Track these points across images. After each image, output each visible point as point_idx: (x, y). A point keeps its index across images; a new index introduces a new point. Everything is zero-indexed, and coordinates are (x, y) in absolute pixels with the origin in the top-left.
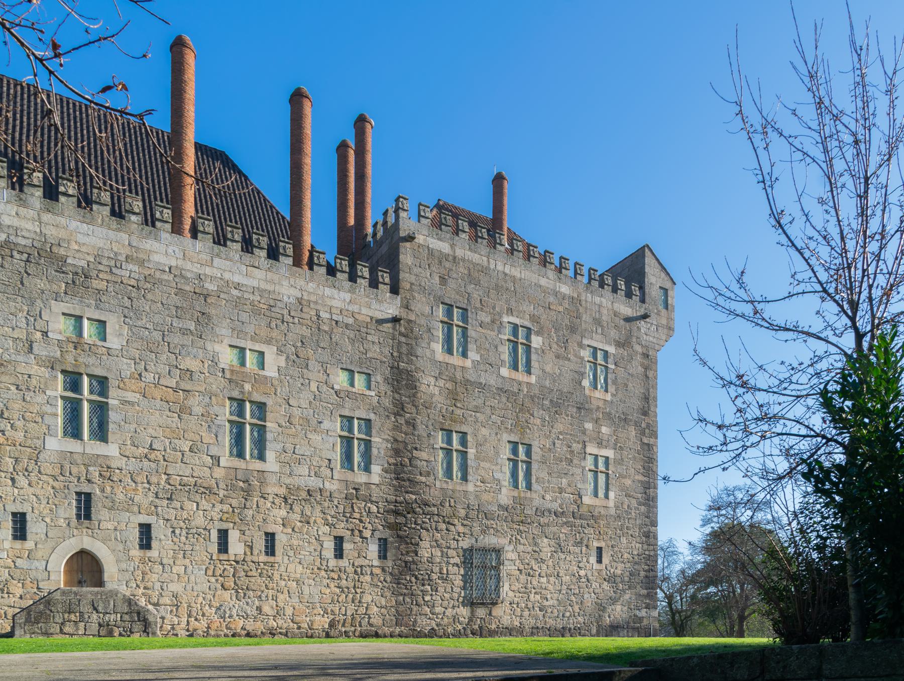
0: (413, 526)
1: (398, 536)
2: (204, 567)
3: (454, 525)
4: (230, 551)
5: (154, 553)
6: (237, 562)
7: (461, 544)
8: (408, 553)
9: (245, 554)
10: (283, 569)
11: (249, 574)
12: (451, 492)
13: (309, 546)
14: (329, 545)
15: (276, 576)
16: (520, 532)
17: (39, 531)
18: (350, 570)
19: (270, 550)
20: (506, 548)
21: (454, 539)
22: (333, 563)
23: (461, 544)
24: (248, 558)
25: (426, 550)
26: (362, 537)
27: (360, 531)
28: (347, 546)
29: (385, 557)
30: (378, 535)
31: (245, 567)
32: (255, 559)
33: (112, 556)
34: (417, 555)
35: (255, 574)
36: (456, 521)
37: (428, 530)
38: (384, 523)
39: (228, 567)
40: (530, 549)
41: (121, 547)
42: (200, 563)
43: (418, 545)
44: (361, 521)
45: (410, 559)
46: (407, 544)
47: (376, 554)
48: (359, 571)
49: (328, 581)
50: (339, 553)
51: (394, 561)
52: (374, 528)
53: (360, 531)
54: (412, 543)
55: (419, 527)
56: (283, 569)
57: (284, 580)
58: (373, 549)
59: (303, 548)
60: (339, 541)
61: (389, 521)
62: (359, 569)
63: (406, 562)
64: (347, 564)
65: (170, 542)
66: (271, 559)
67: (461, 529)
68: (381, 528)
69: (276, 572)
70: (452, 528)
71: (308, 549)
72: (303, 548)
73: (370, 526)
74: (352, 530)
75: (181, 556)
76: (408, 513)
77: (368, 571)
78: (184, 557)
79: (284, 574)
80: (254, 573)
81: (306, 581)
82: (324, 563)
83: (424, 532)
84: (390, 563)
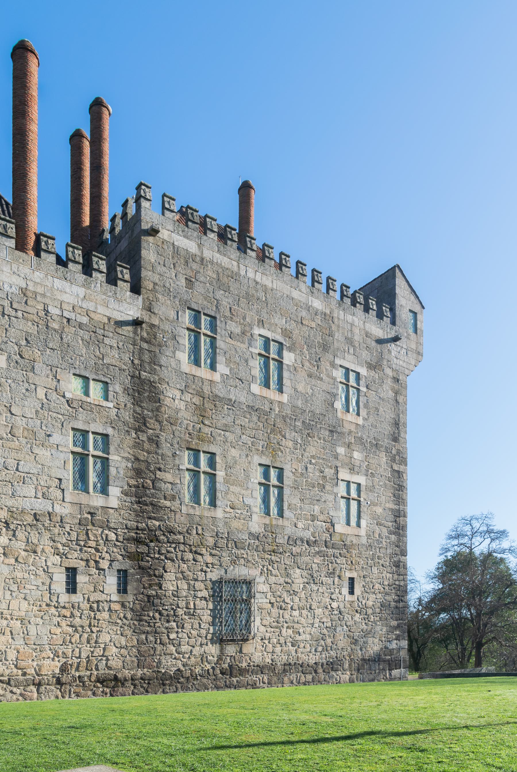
0: (157, 556)
1: (140, 567)
3: (202, 555)
7: (209, 575)
8: (150, 585)
12: (198, 519)
13: (36, 579)
14: (60, 578)
16: (271, 562)
18: (85, 606)
20: (258, 580)
21: (202, 570)
22: (64, 598)
23: (209, 575)
25: (171, 582)
26: (98, 569)
27: (96, 562)
28: (81, 579)
29: (125, 591)
30: (116, 566)
34: (161, 588)
36: (204, 551)
37: (173, 561)
38: (124, 553)
40: (282, 580)
43: (162, 577)
44: (97, 550)
45: (154, 593)
46: (150, 576)
47: (115, 588)
48: (95, 607)
50: (72, 587)
51: (135, 595)
52: (113, 559)
53: (96, 562)
54: (155, 575)
55: (163, 557)
58: (111, 582)
59: (29, 582)
60: (72, 573)
61: (129, 550)
62: (95, 606)
63: (149, 597)
64: (81, 599)
67: (209, 559)
68: (120, 558)
70: (199, 558)
72: (29, 582)
73: (107, 556)
74: (87, 561)
76: (151, 541)
77: (106, 606)
79: (5, 612)
81: (32, 620)
82: (54, 599)
83: (169, 563)
84: (130, 598)
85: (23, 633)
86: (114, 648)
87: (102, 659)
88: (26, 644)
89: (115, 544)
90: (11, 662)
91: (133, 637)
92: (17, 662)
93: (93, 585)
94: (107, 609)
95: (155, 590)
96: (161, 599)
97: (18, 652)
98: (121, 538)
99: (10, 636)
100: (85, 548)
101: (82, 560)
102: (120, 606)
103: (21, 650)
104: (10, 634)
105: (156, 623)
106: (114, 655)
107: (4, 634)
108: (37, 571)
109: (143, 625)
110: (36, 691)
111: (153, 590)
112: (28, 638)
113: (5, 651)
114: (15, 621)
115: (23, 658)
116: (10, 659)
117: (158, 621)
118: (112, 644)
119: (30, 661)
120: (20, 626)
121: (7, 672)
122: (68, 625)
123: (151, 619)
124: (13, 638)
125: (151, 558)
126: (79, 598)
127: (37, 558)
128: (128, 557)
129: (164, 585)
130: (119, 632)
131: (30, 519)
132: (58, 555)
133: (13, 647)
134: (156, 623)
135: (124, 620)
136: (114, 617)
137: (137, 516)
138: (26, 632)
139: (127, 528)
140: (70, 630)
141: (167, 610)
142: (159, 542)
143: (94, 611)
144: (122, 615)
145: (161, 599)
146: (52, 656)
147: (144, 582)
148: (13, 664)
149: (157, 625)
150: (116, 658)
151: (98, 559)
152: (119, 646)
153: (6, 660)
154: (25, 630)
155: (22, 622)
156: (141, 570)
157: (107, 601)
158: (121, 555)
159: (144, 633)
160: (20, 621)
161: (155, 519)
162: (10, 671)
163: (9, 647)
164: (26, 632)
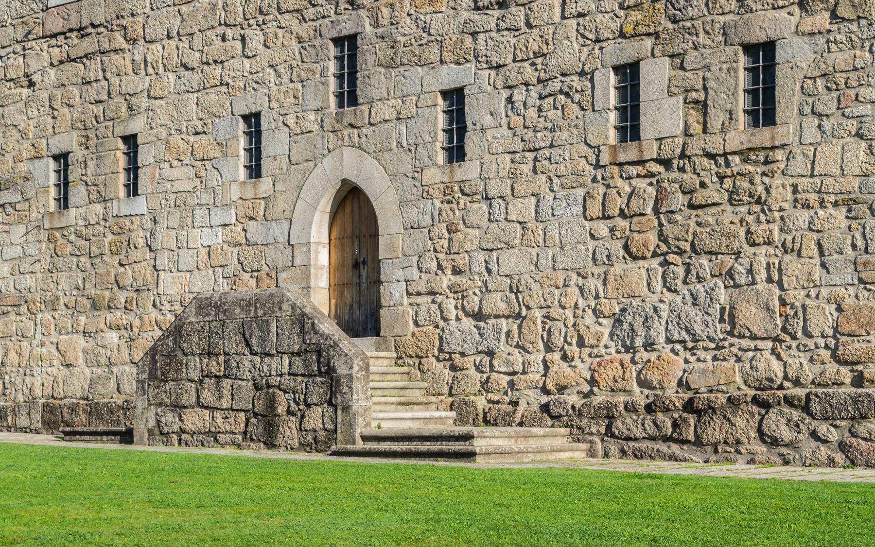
2: (580, 193)
4: (647, 131)
5: (469, 171)
6: (666, 163)
9: (687, 133)
10: (800, 165)
11: (699, 198)
15: (781, 196)
17: (279, 151)
19: (763, 109)
24: (695, 147)
31: (689, 178)
32: (715, 144)
33: (392, 192)
35: (717, 198)
39: (641, 184)
41: (407, 164)
42: (567, 182)
56: (800, 165)
57: (807, 206)
65: (504, 131)
66: (764, 136)
69: (778, 181)
75: (526, 169)
78: (535, 171)
80: (712, 194)
85: (854, 247)
88: (861, 281)
90: (821, 342)
92: (837, 340)
97: (839, 309)
99: (817, 260)
103: (849, 301)
104: (815, 252)
107: (799, 255)
112: (866, 264)
113: (804, 307)
114: (831, 210)
115: (853, 327)
116: (816, 332)
120: (845, 223)
121: (810, 372)
124: (823, 265)
133: (825, 292)
138: (860, 243)
148: (827, 347)
153: (808, 335)
154: (858, 236)
155: (849, 211)
160: (844, 210)
162: (818, 368)
163: (813, 293)
164: (860, 243)
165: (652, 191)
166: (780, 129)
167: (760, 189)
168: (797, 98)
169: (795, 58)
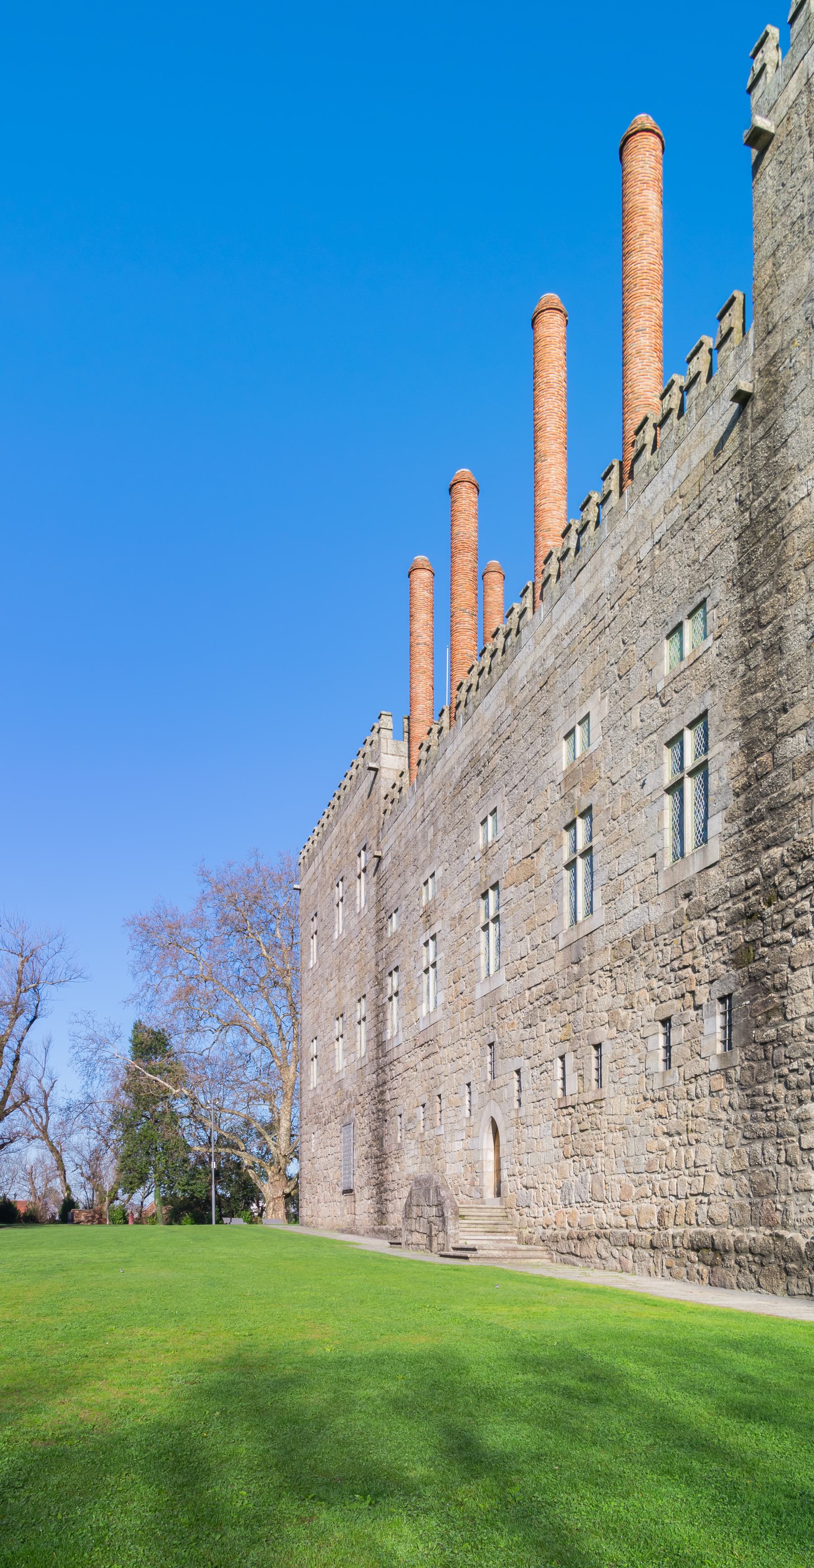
0: (777, 936)
8: (768, 1015)
30: (719, 990)
45: (772, 1032)
49: (656, 1122)
51: (743, 1047)
68: (721, 969)
71: (632, 1062)
84: (738, 1054)
86: (718, 1175)
87: (701, 1202)
89: (716, 944)
91: (743, 1149)
93: (689, 1043)
94: (706, 1092)
95: (776, 1025)
96: (785, 1045)
98: (722, 925)
100: (680, 972)
101: (676, 998)
102: (723, 1080)
105: (776, 1109)
106: (717, 1193)
108: (635, 1039)
109: (754, 1119)
110: (631, 1257)
111: (771, 1027)
117: (782, 1103)
118: (714, 1168)
119: (630, 1202)
122: (664, 1133)
123: (770, 1102)
125: (768, 945)
126: (673, 1077)
127: (634, 1016)
128: (733, 961)
129: (789, 1007)
130: (722, 1140)
131: (627, 950)
132: (653, 1000)
134: (776, 1109)
135: (730, 1110)
136: (716, 1107)
137: (746, 857)
139: (732, 896)
140: (667, 1141)
141: (797, 1070)
142: (782, 898)
143: (692, 1100)
144: (726, 1099)
145: (785, 1045)
146: (650, 1193)
147: (756, 1011)
149: (779, 1113)
150: (719, 1198)
151: (694, 988)
152: (722, 1170)
156: (753, 984)
157: (706, 1074)
158: (724, 963)
159: (759, 1137)
161: (775, 843)
165: (570, 1121)
166: (603, 1089)
167: (598, 1121)
168: (608, 1073)
169: (606, 1049)
